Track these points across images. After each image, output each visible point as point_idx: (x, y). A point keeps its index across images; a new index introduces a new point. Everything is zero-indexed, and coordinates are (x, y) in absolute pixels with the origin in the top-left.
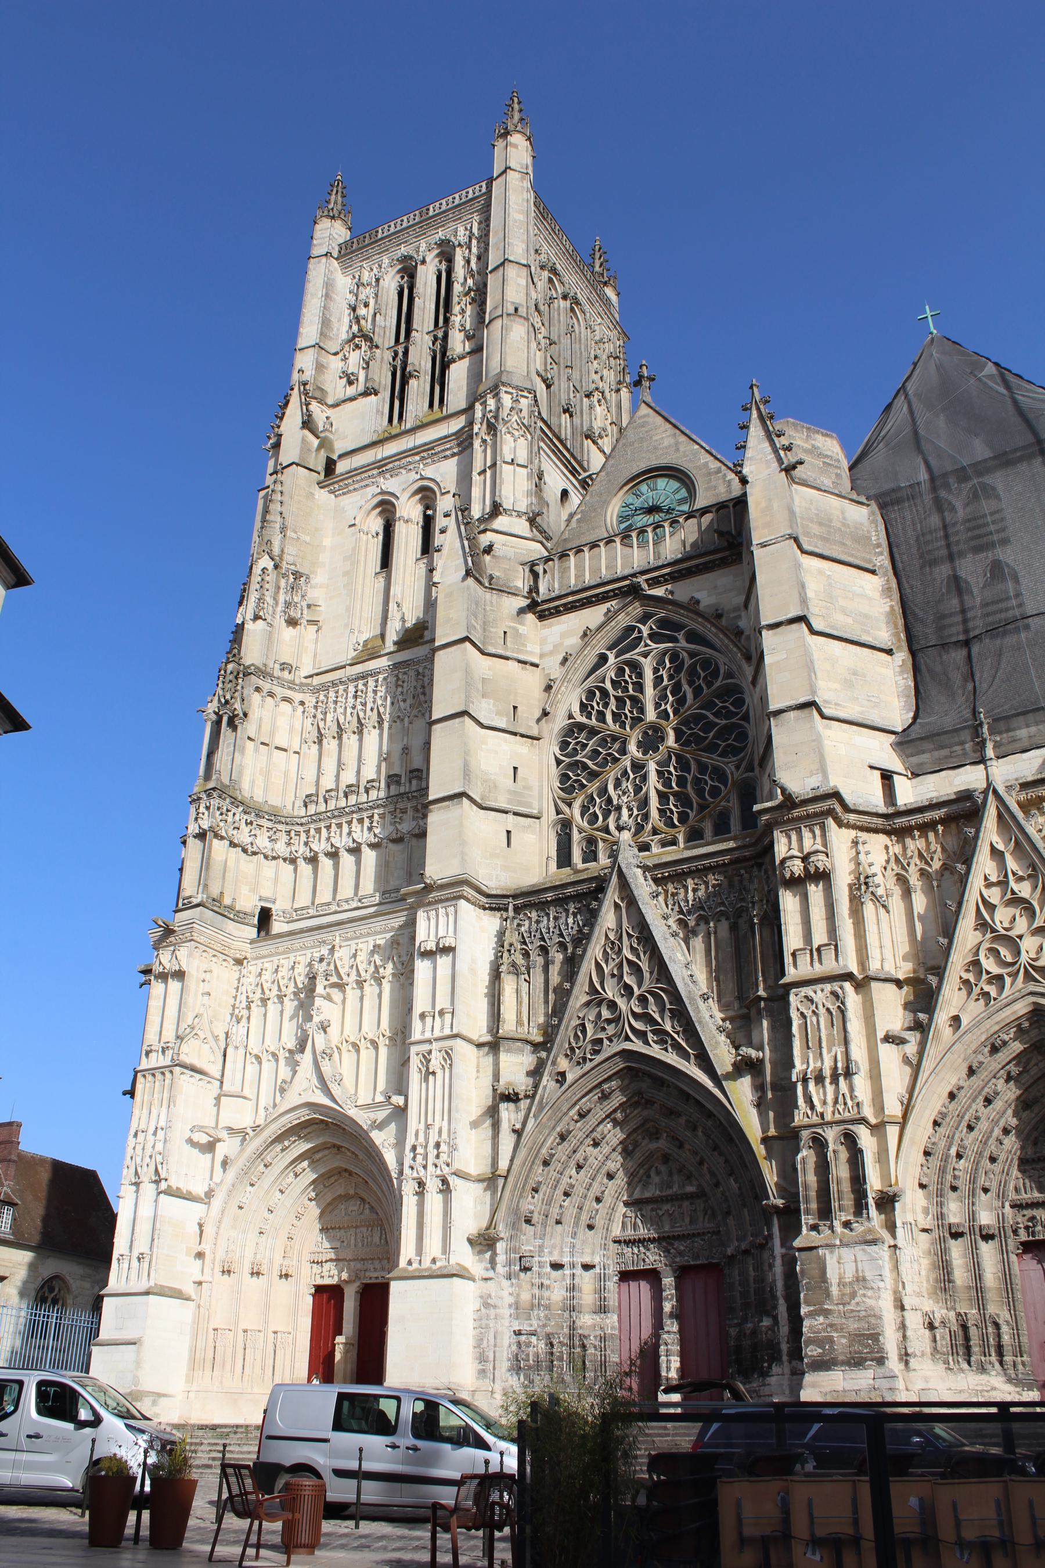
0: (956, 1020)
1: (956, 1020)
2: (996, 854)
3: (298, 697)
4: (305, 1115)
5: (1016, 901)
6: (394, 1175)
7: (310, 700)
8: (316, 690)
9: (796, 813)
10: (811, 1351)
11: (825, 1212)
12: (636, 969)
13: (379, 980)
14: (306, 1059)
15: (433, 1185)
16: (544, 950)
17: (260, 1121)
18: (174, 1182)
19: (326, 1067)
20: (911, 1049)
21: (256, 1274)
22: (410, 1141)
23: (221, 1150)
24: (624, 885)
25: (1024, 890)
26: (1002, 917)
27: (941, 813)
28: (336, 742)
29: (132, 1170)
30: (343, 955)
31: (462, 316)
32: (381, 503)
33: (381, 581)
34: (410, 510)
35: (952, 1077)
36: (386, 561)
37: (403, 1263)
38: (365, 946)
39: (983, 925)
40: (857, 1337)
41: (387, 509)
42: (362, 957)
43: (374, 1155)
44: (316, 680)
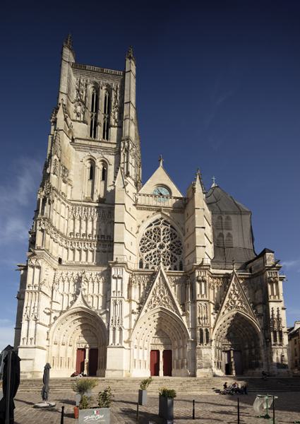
0: (224, 313)
1: (224, 313)
2: (233, 285)
3: (67, 205)
4: (80, 310)
5: (236, 294)
6: (106, 325)
7: (71, 207)
8: (72, 204)
9: (202, 267)
10: (198, 366)
11: (202, 342)
12: (164, 292)
13: (98, 282)
14: (80, 297)
15: (117, 328)
16: (139, 285)
17: (64, 309)
18: (41, 321)
19: (85, 299)
20: (215, 316)
21: (63, 345)
22: (111, 319)
23: (53, 315)
24: (162, 274)
25: (237, 292)
26: (233, 296)
27: (222, 276)
28: (72, 221)
29: (34, 317)
30: (88, 274)
31: (115, 114)
32: (90, 159)
33: (90, 183)
34: (99, 165)
35: (221, 322)
36: (92, 176)
37: (110, 344)
38: (94, 273)
39: (230, 297)
40: (207, 364)
41: (92, 161)
42: (93, 275)
43: (99, 321)
44: (72, 202)
